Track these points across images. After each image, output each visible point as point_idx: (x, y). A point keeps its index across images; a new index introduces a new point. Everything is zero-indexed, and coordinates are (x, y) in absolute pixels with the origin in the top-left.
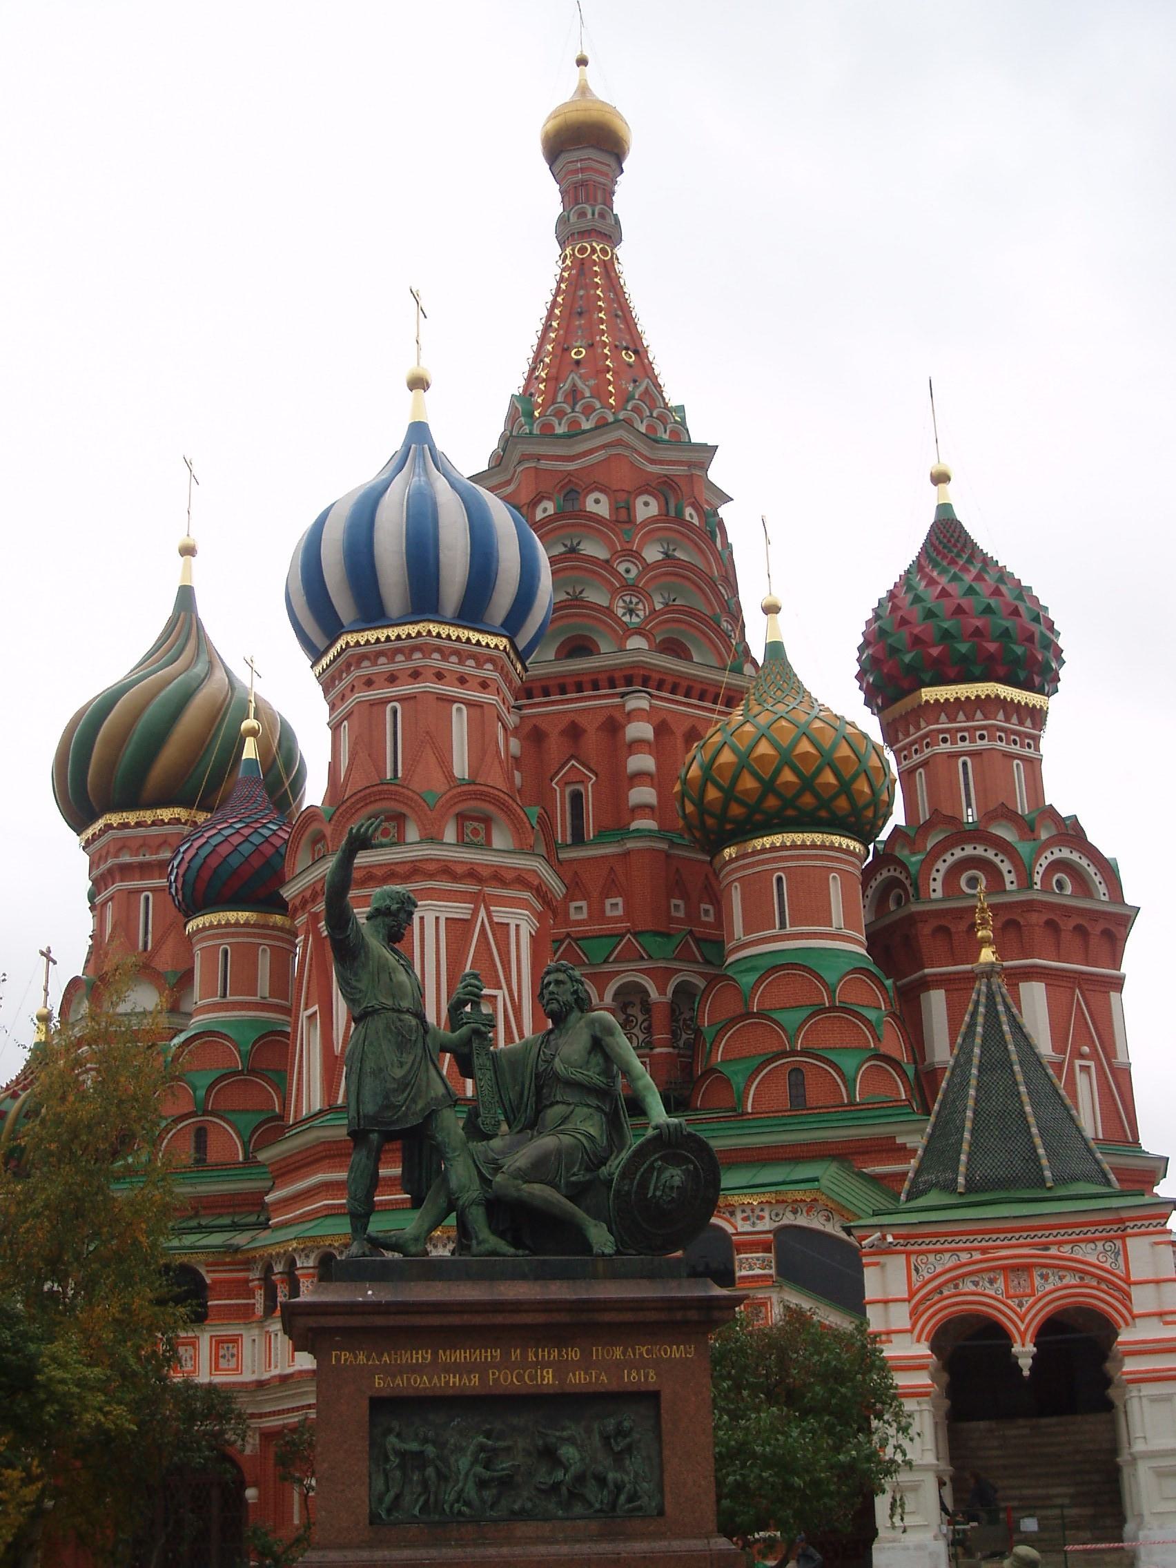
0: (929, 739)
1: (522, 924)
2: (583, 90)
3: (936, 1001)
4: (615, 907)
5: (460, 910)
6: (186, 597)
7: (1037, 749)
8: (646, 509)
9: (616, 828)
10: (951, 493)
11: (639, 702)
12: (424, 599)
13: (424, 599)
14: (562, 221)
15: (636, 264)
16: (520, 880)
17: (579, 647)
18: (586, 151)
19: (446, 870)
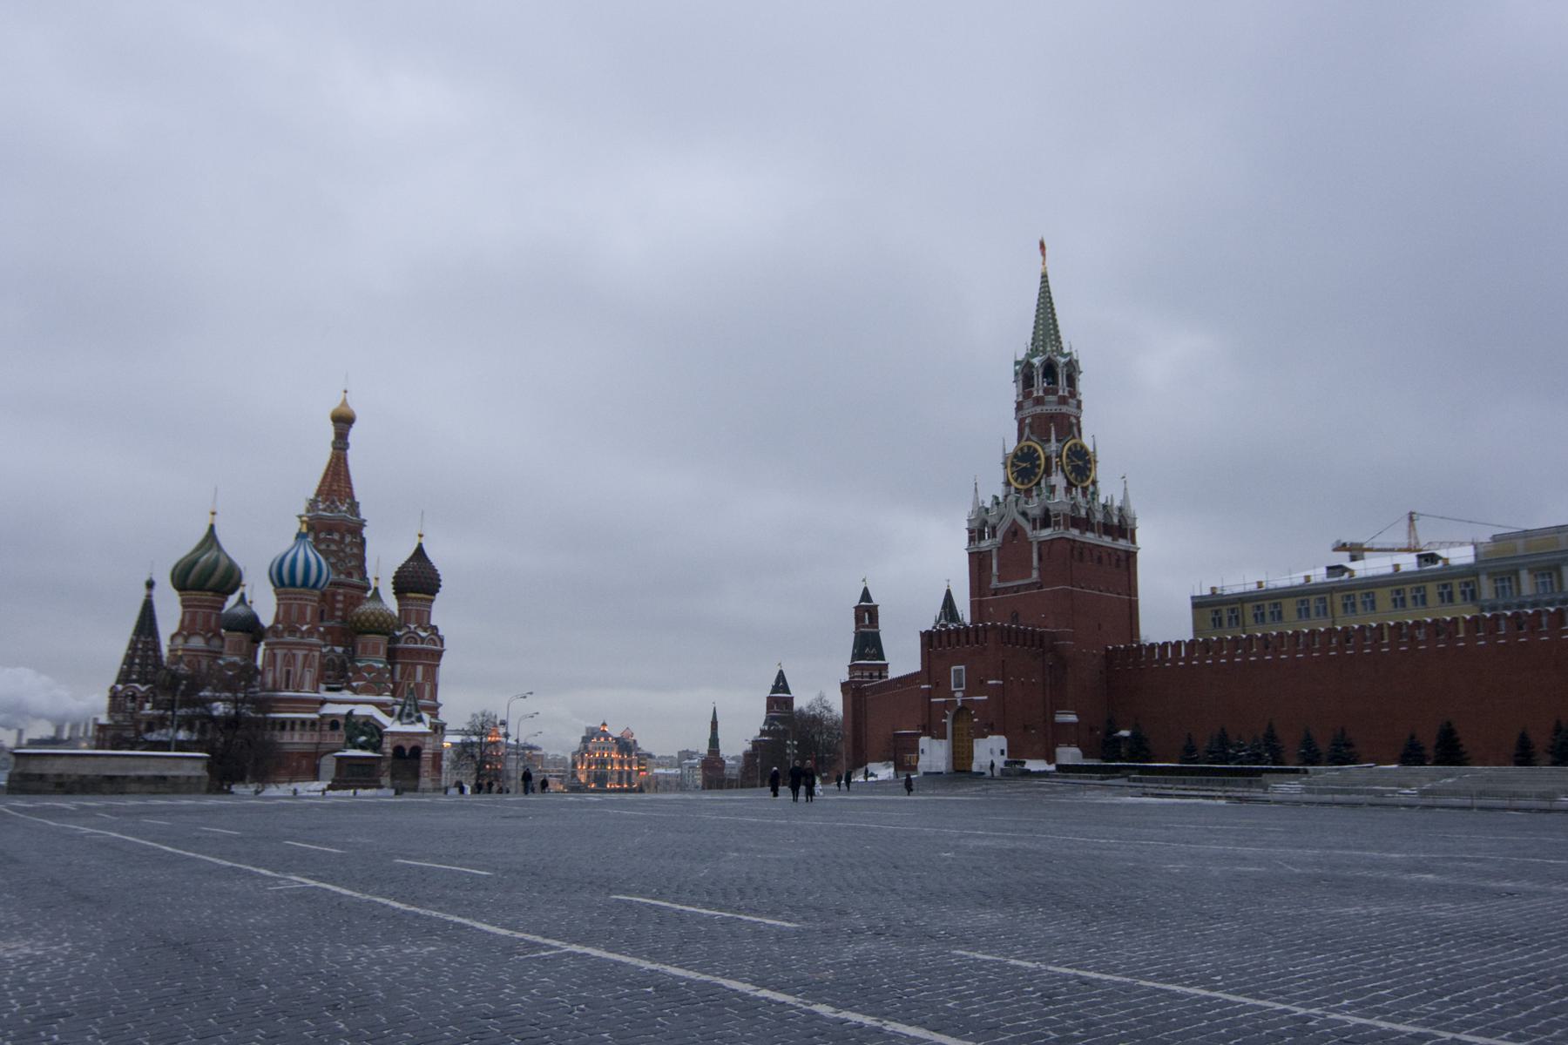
2: (344, 403)
3: (398, 667)
6: (212, 527)
8: (348, 539)
10: (423, 540)
14: (334, 443)
18: (343, 422)
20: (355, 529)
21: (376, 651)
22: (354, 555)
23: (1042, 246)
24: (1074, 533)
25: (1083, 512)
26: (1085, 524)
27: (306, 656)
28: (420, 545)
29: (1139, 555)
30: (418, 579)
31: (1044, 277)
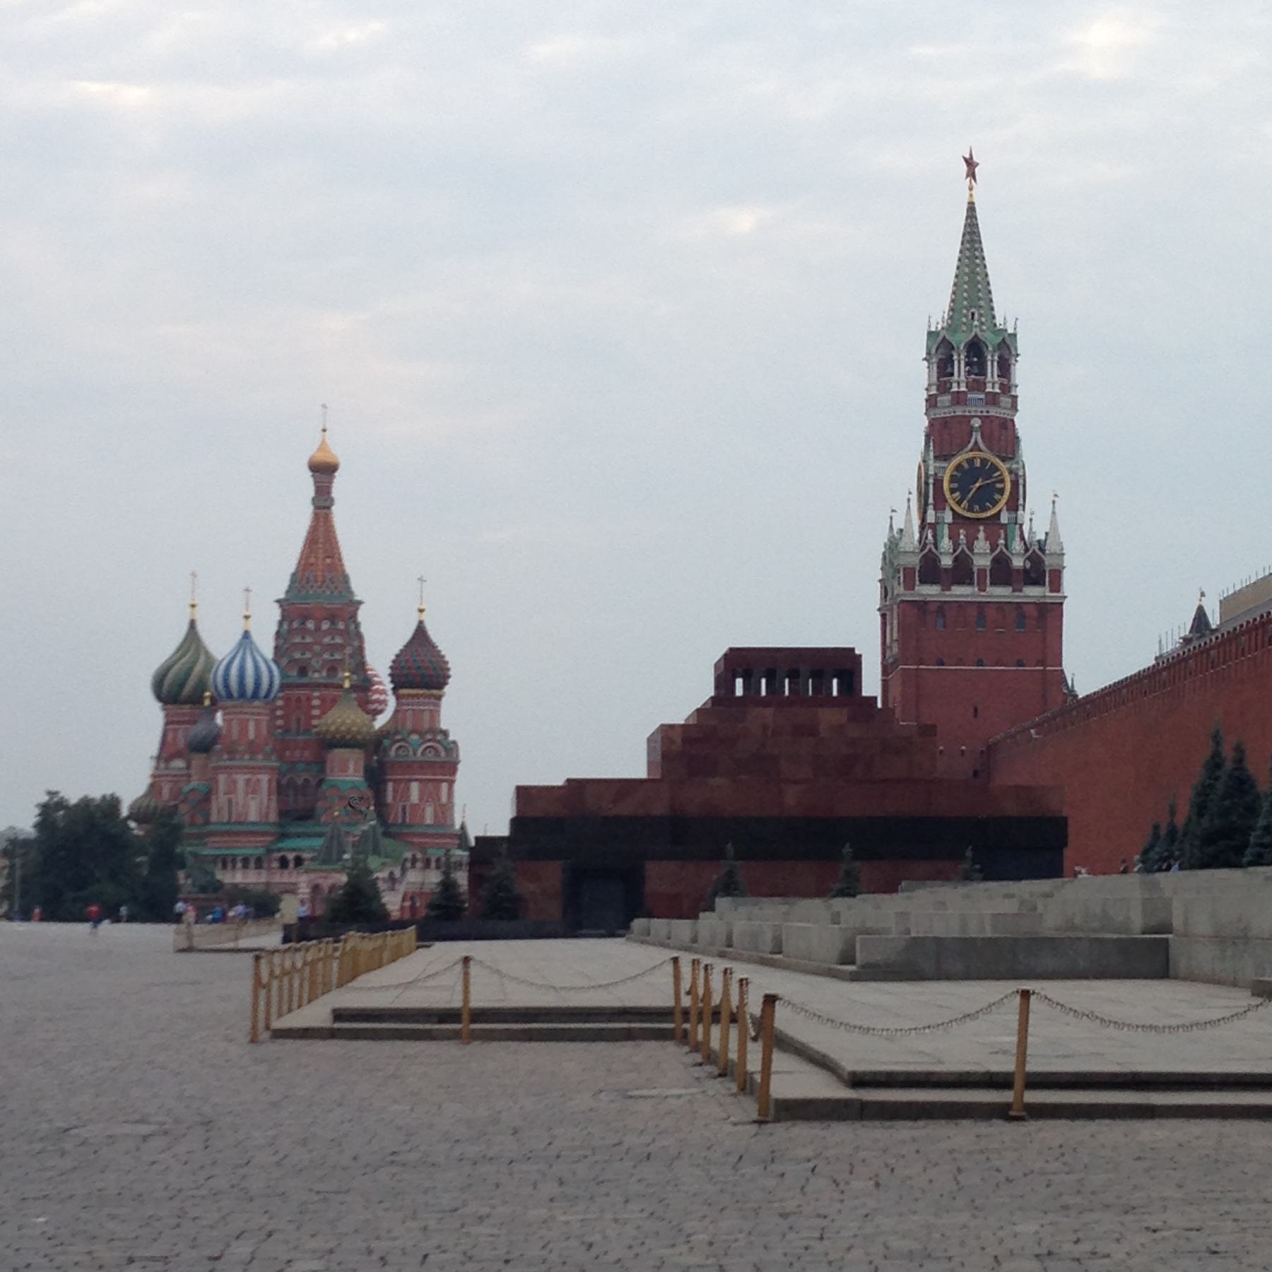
0: (403, 704)
1: (264, 778)
2: (323, 447)
3: (390, 786)
4: (307, 754)
5: (247, 777)
6: (192, 624)
7: (438, 706)
9: (307, 730)
10: (424, 617)
11: (316, 694)
12: (242, 694)
13: (242, 694)
15: (340, 516)
16: (265, 767)
17: (303, 671)
18: (323, 471)
19: (246, 767)
20: (343, 613)
21: (344, 769)
22: (333, 648)
23: (970, 163)
24: (930, 591)
25: (947, 561)
26: (962, 572)
27: (248, 781)
28: (421, 622)
29: (1064, 606)
30: (422, 670)
31: (971, 208)
